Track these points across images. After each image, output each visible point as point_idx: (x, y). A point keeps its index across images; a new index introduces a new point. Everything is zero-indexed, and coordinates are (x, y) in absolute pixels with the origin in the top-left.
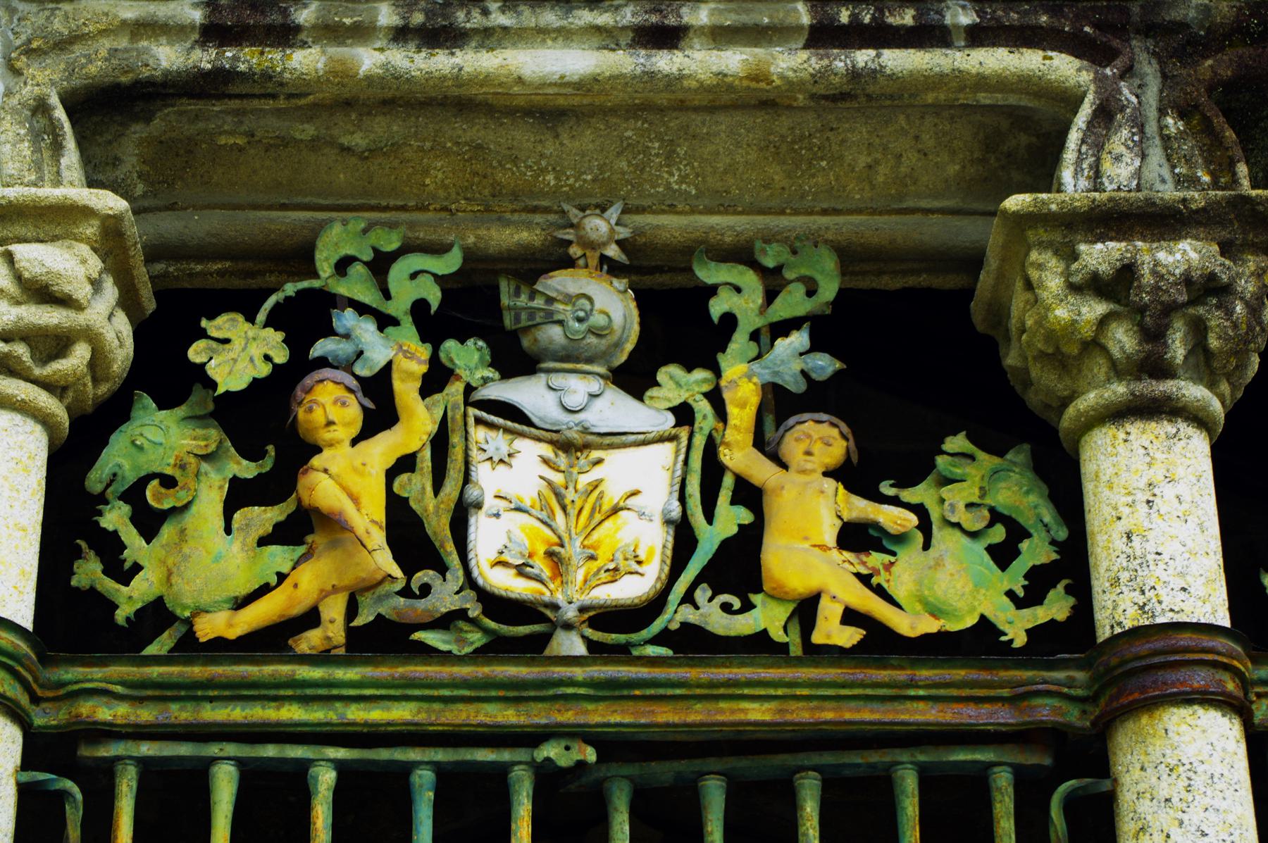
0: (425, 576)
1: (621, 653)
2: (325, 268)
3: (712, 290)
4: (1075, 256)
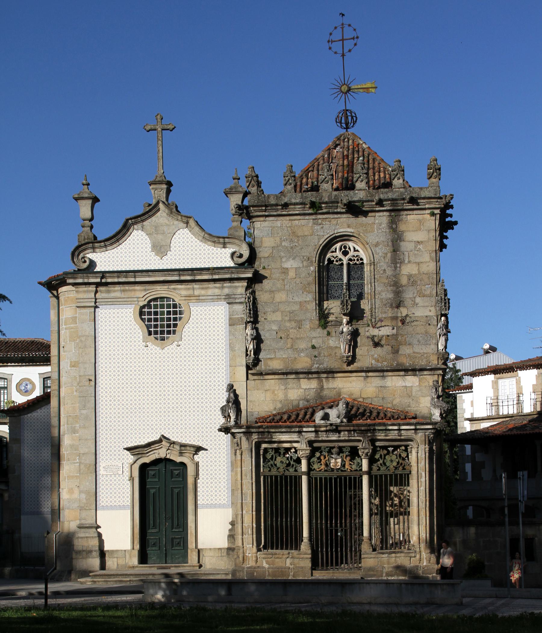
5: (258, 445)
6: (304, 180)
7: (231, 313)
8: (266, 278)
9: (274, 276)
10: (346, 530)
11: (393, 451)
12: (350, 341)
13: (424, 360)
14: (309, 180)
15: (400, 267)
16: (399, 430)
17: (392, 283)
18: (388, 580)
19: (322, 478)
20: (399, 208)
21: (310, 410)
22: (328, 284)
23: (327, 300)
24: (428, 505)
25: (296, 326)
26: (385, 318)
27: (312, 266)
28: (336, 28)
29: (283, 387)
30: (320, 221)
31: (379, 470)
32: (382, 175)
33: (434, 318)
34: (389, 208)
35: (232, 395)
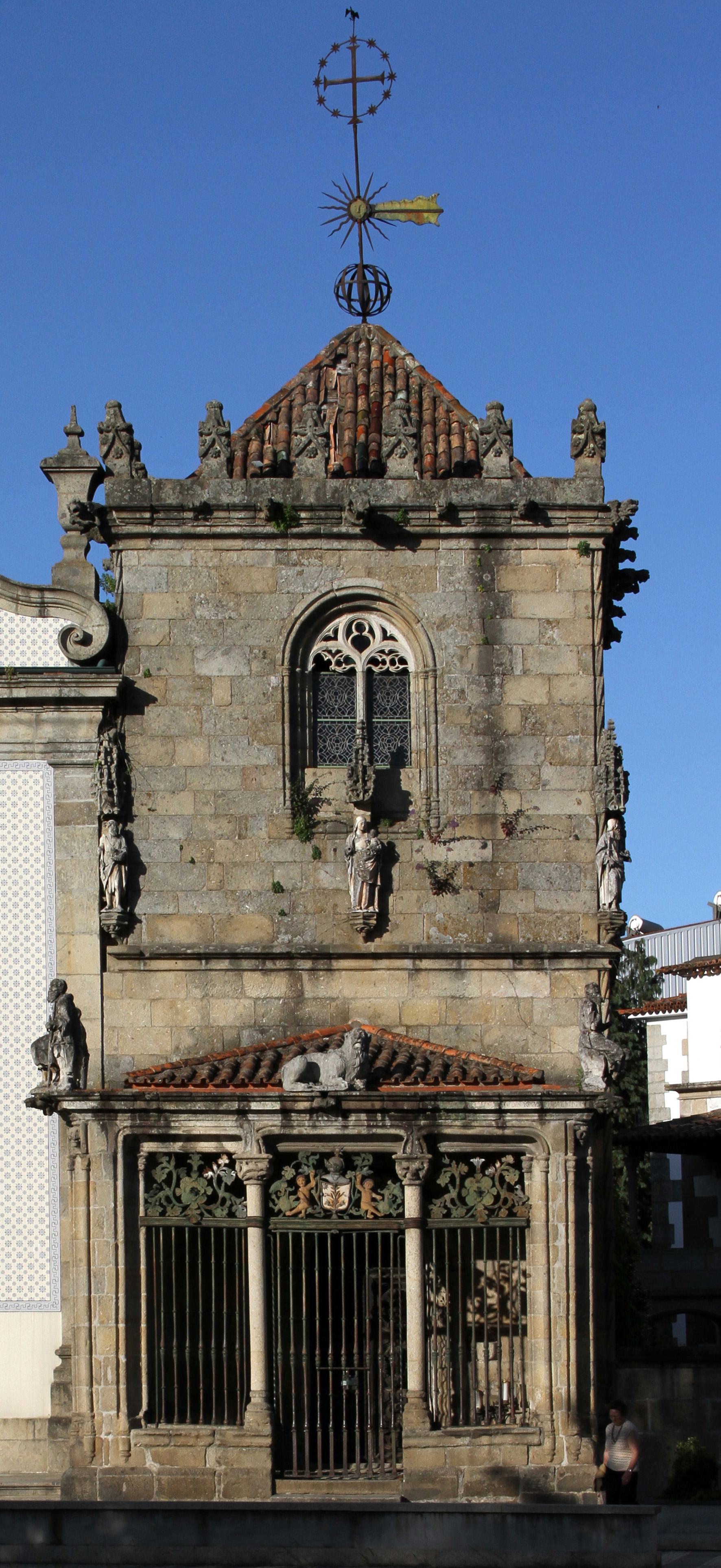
5: (132, 1145)
6: (254, 446)
7: (60, 791)
8: (153, 700)
9: (173, 697)
10: (362, 1375)
11: (484, 1167)
12: (374, 874)
14: (267, 446)
15: (502, 686)
16: (500, 1112)
17: (482, 726)
18: (470, 1505)
19: (300, 1234)
20: (499, 529)
21: (270, 1055)
22: (316, 723)
23: (314, 765)
24: (572, 1311)
25: (233, 832)
26: (463, 817)
27: (274, 672)
28: (335, 48)
29: (197, 993)
30: (294, 556)
31: (448, 1215)
32: (455, 442)
34: (473, 529)
35: (63, 1010)
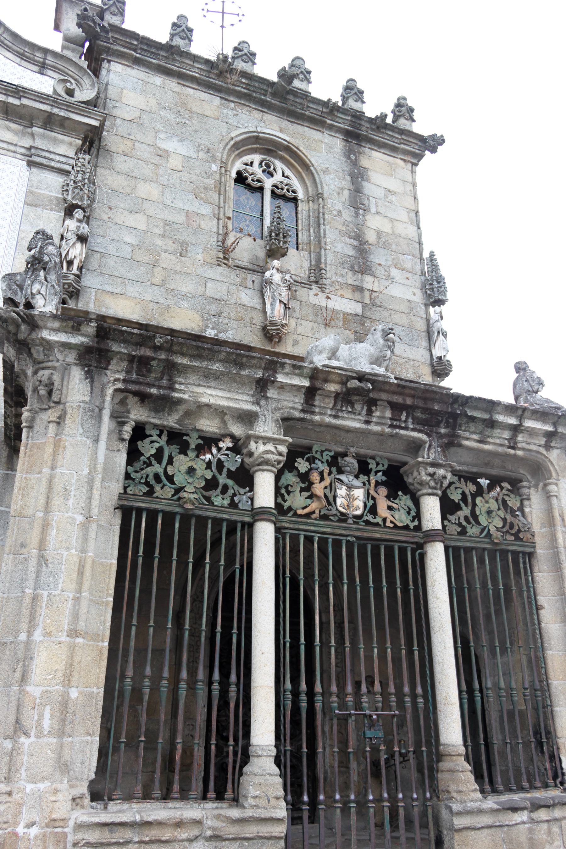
0: (330, 507)
1: (357, 523)
2: (314, 452)
3: (369, 464)
4: (426, 469)
13: (411, 371)
17: (353, 234)
27: (215, 162)
33: (420, 308)
